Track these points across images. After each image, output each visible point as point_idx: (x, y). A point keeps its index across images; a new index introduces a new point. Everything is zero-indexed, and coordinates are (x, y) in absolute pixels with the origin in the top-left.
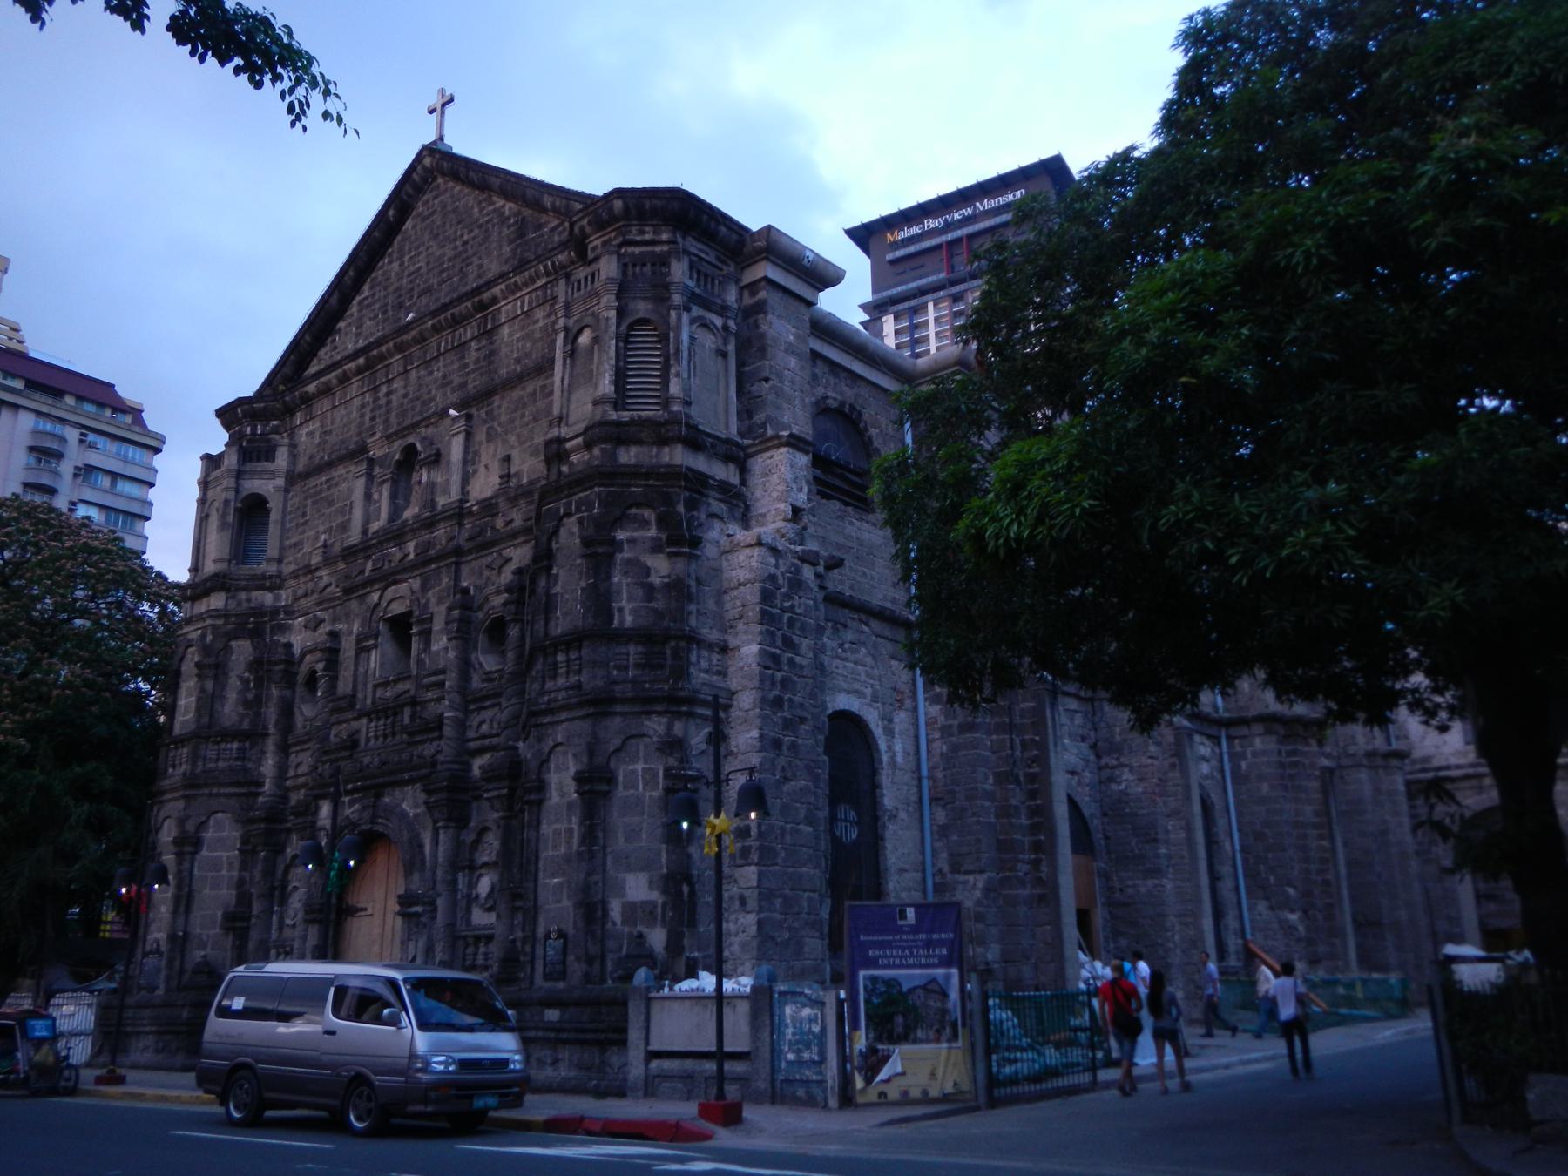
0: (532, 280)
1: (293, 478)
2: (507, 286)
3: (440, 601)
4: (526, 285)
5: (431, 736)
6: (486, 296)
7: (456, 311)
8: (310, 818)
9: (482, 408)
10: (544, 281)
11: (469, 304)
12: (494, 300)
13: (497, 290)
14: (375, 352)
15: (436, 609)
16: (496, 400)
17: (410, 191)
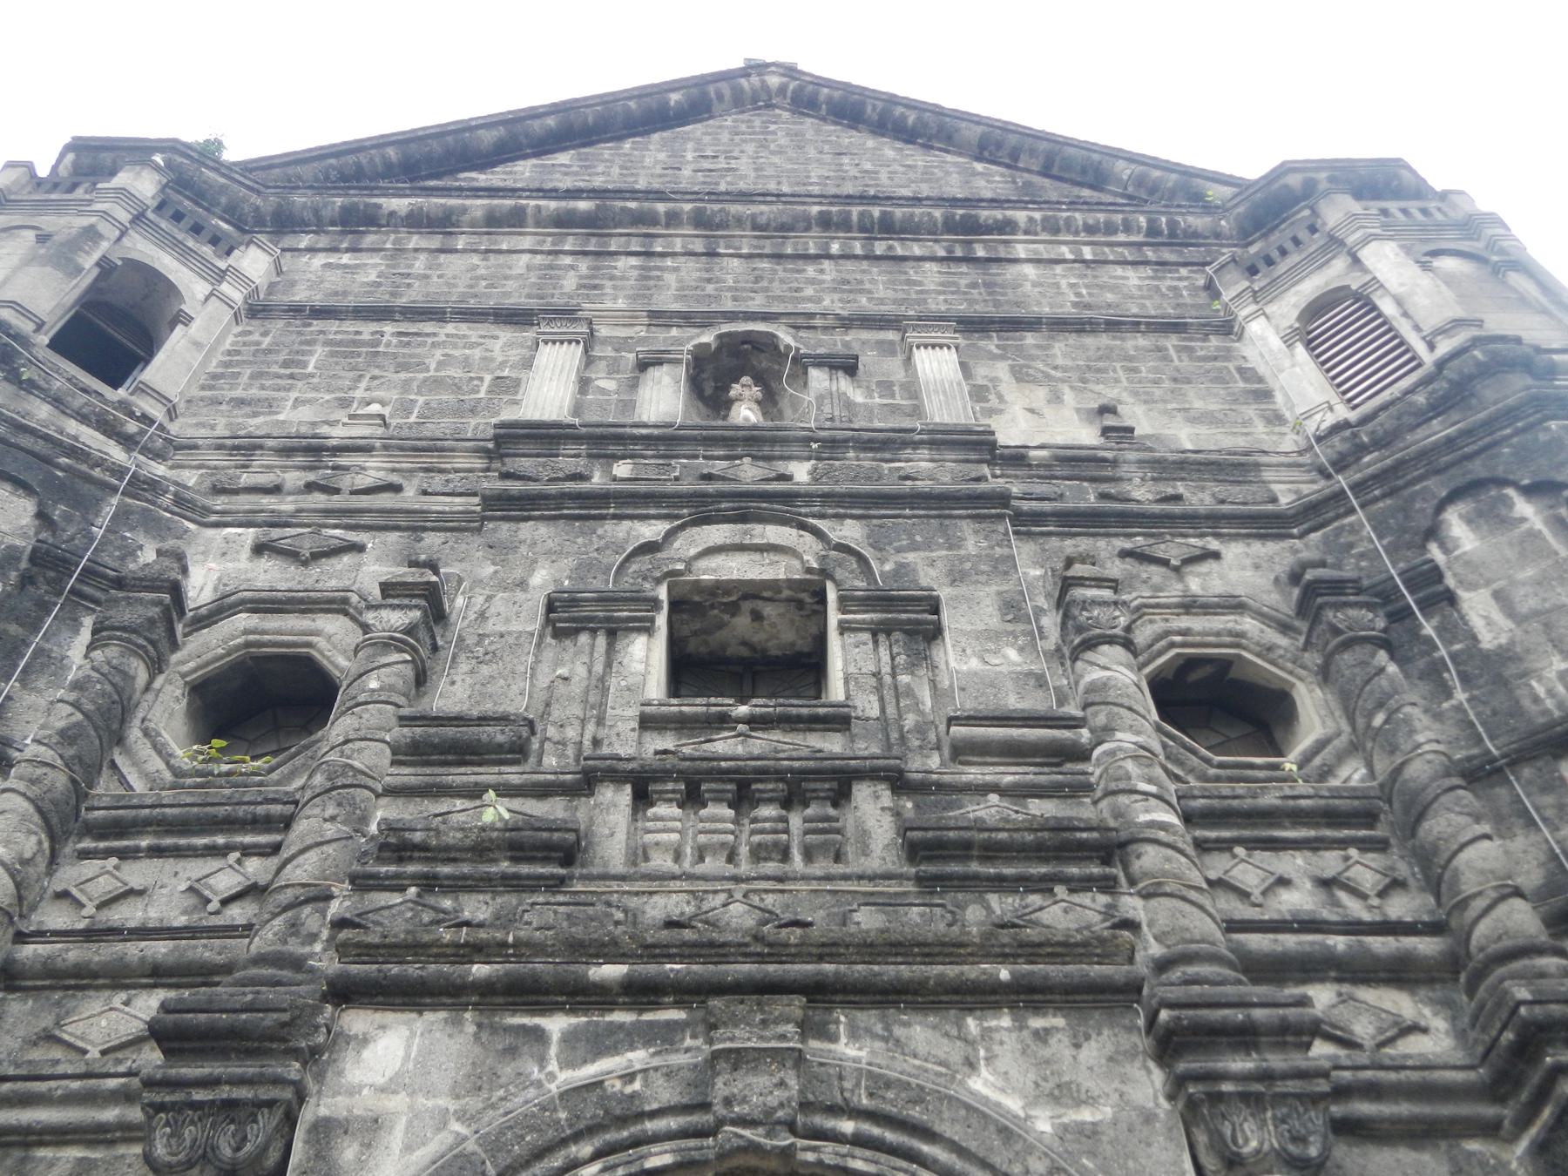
0: (1110, 229)
1: (256, 310)
2: (1045, 219)
3: (957, 577)
4: (1090, 229)
5: (1074, 870)
6: (985, 214)
7: (898, 213)
8: (293, 1069)
9: (990, 338)
10: (1133, 238)
11: (938, 214)
12: (1007, 226)
13: (1021, 216)
14: (633, 205)
15: (944, 593)
16: (1030, 339)
17: (727, 92)
